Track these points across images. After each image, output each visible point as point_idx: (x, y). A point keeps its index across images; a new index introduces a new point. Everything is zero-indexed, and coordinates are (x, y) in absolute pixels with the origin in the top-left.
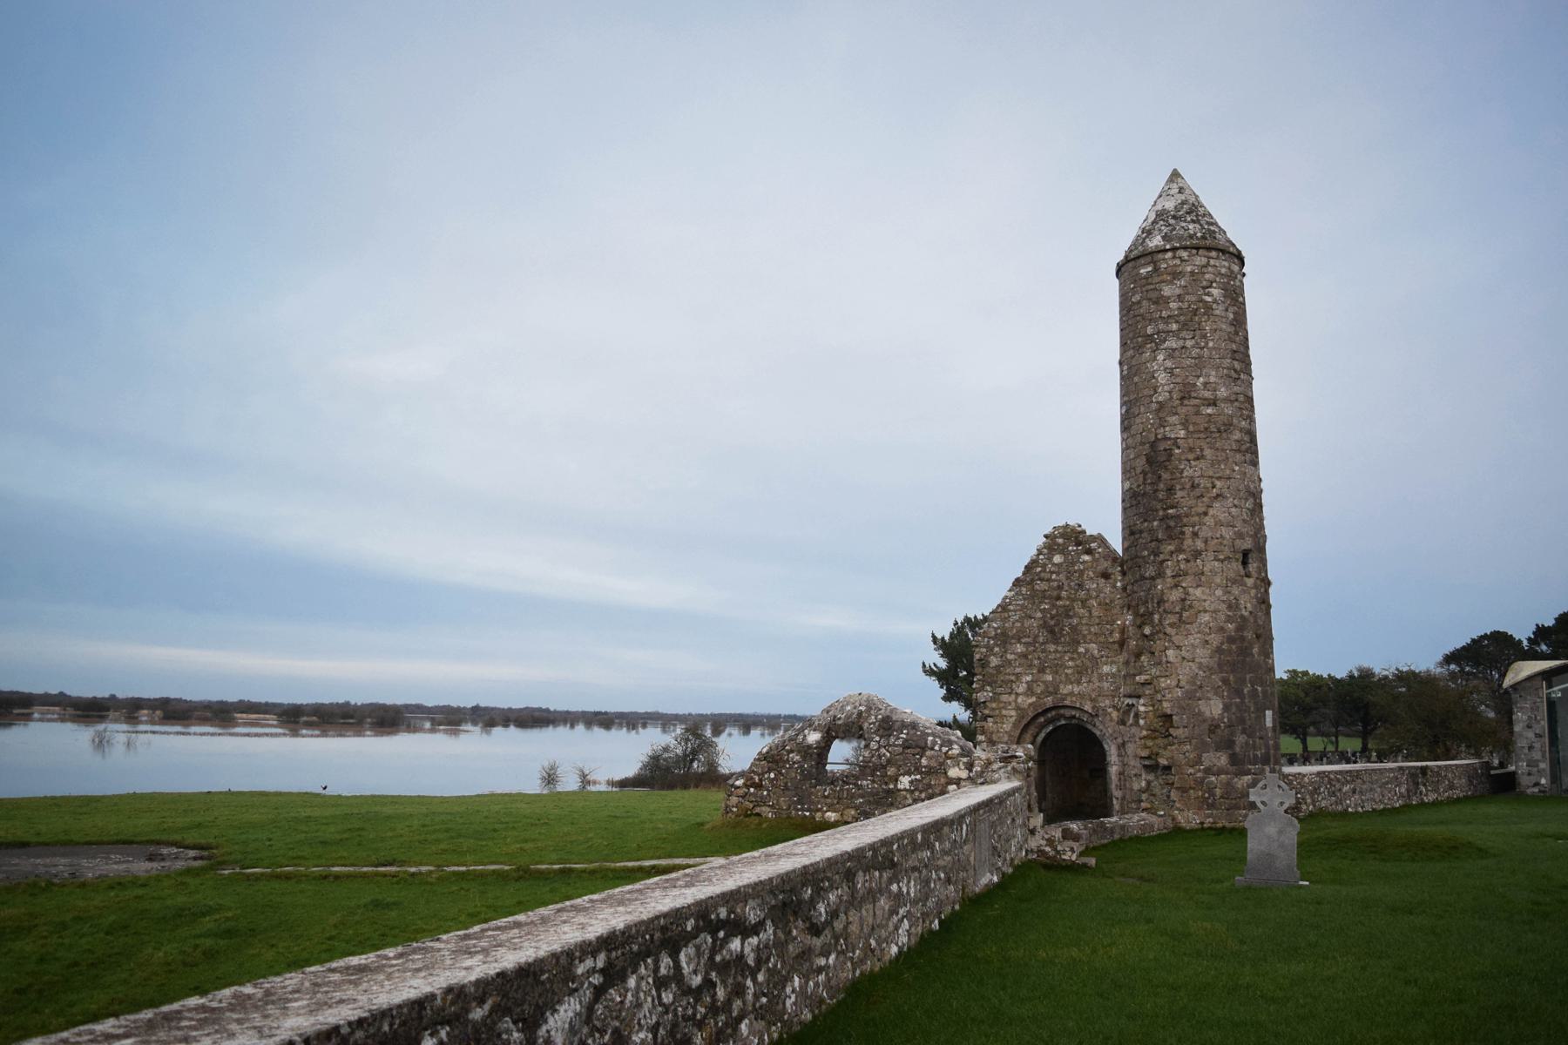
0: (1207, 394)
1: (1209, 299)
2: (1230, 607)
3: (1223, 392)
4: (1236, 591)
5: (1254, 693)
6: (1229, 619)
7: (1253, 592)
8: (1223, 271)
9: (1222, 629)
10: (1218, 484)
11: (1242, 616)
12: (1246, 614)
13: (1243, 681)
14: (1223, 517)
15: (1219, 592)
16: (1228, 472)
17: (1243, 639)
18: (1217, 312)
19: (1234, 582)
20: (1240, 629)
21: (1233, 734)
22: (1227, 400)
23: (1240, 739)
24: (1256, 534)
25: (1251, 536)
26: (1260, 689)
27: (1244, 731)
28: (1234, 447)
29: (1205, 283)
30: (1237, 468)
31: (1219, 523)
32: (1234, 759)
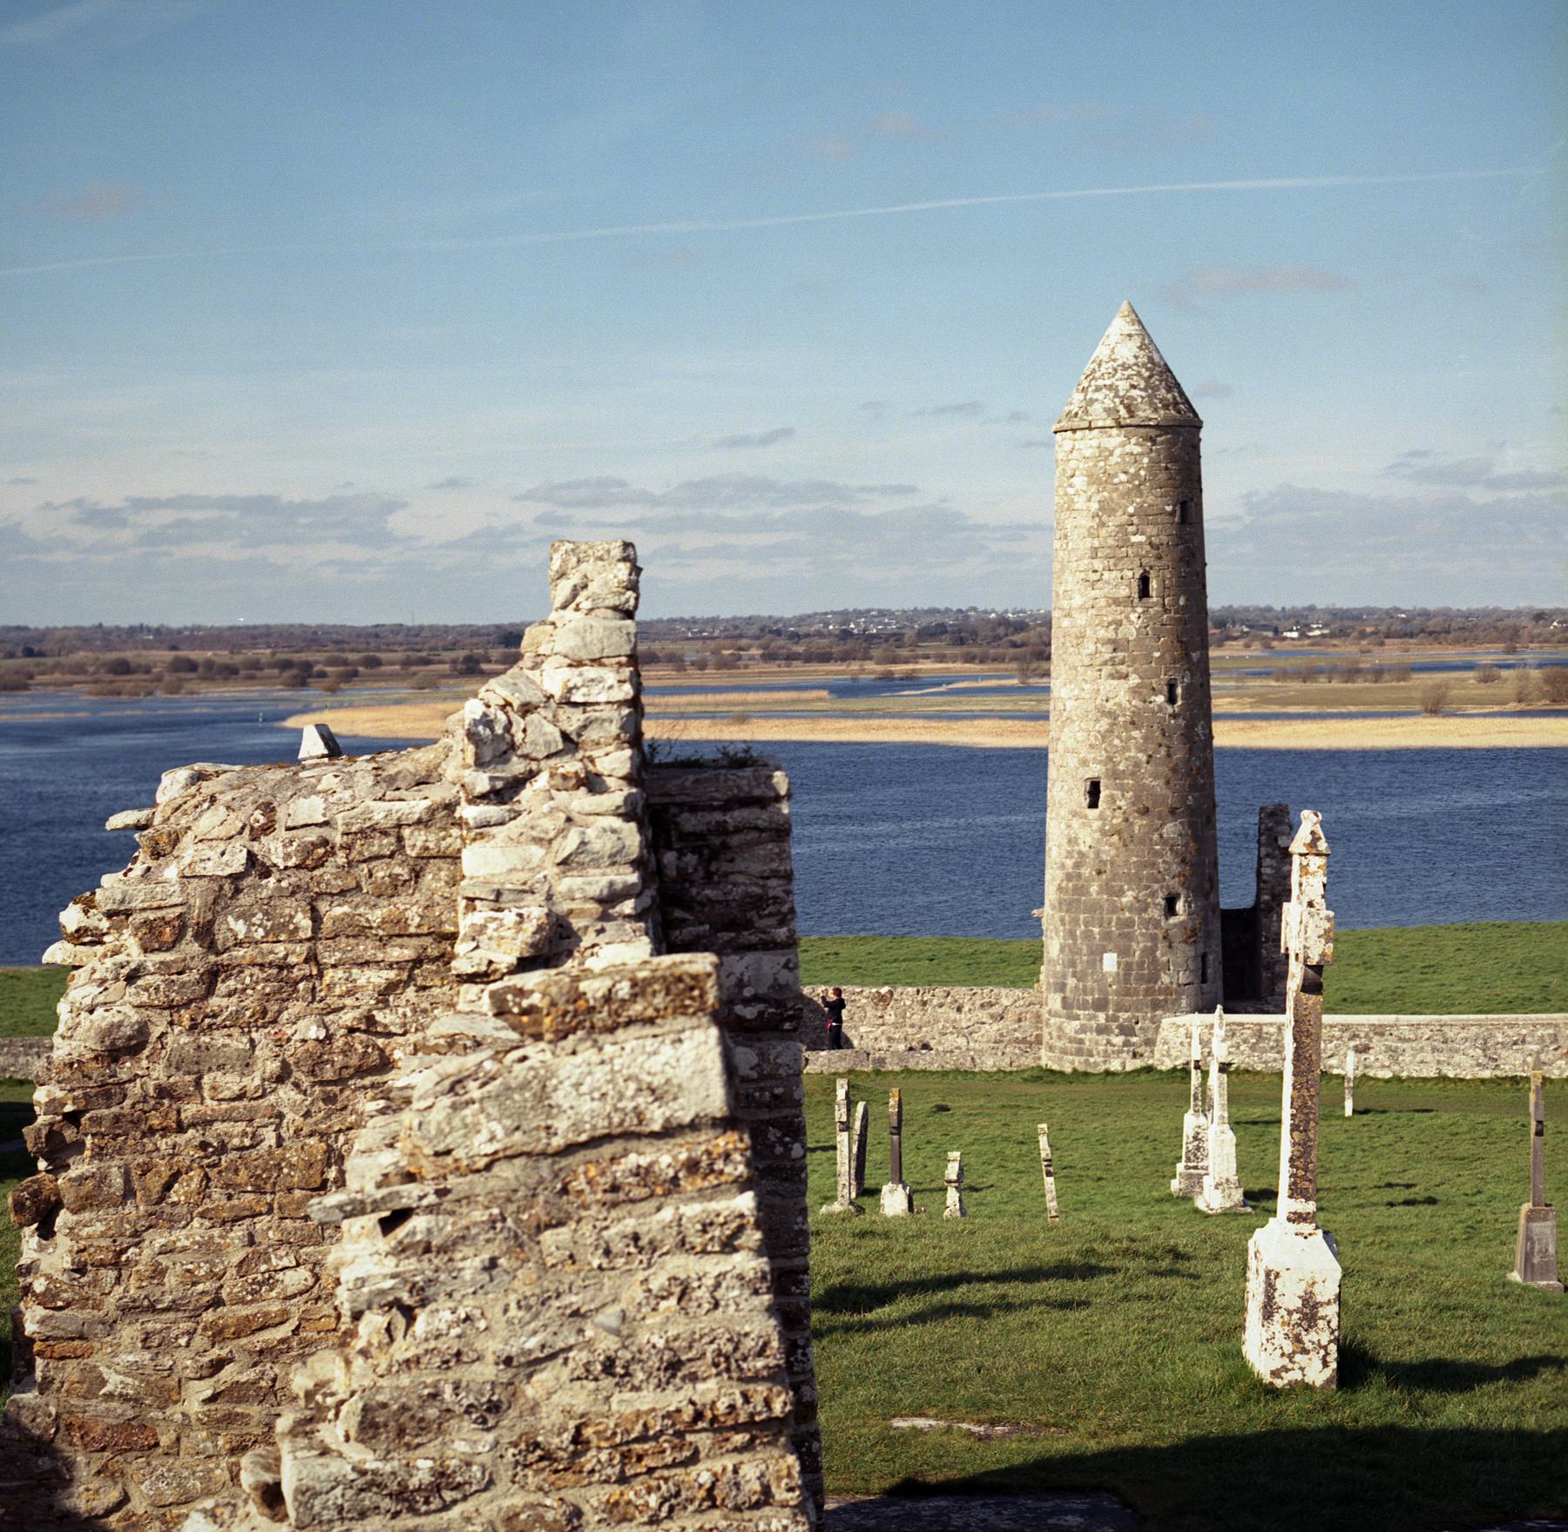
0: (1065, 604)
1: (1071, 491)
2: (1070, 841)
3: (1077, 601)
4: (1076, 823)
5: (1088, 935)
6: (1069, 854)
7: (1097, 825)
8: (1088, 453)
9: (1063, 866)
10: (1070, 704)
11: (1081, 853)
12: (1084, 849)
13: (1075, 922)
14: (1070, 743)
15: (1063, 826)
16: (1076, 692)
17: (1079, 876)
18: (1077, 506)
19: (1075, 814)
20: (1077, 865)
21: (1064, 976)
22: (1083, 608)
23: (1071, 982)
24: (1110, 759)
25: (1100, 762)
26: (1096, 930)
27: (1074, 975)
28: (1087, 662)
29: (1069, 473)
30: (1087, 687)
31: (1067, 751)
32: (1065, 1003)
